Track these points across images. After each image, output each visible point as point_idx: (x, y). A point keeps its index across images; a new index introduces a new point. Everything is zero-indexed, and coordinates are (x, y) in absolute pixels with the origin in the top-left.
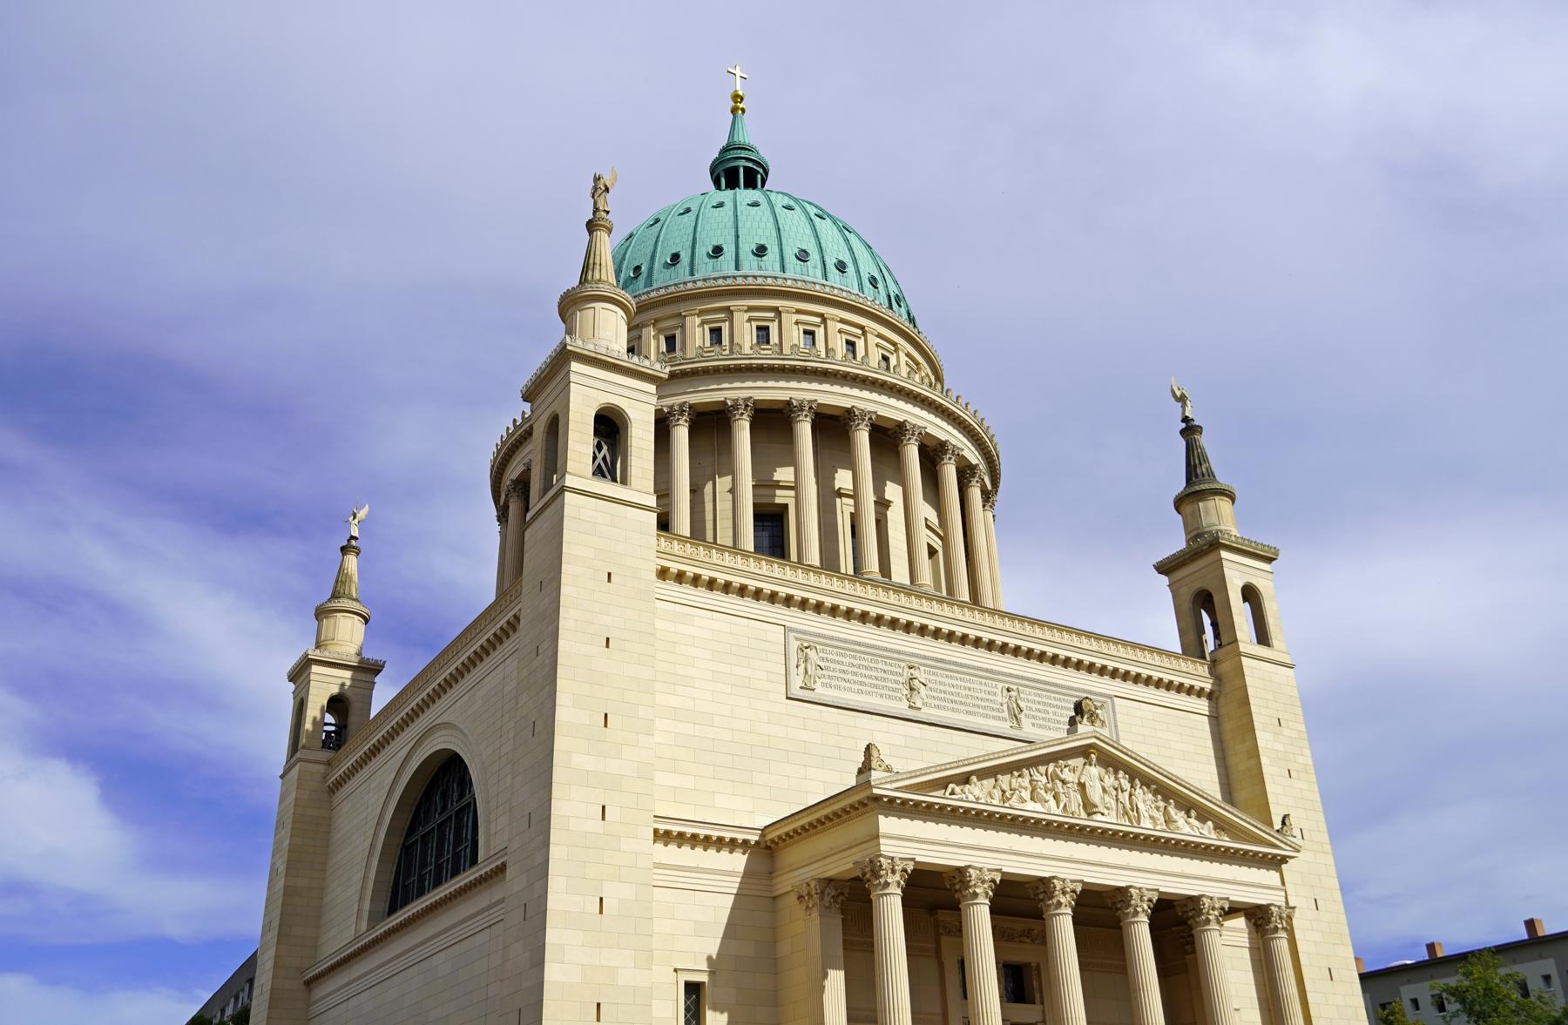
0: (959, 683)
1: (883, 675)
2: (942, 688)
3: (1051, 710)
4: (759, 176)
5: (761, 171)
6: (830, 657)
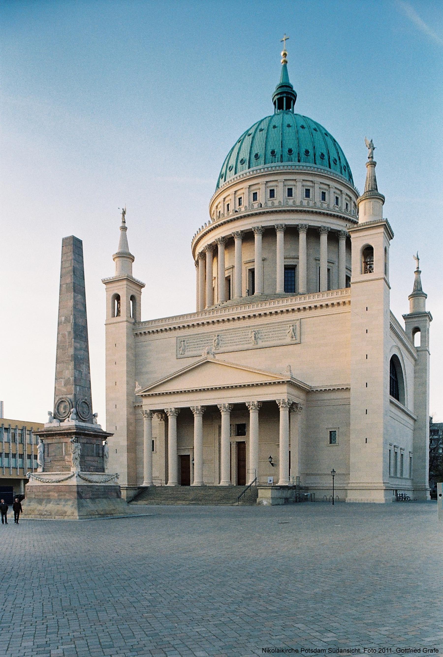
0: (234, 335)
1: (207, 341)
2: (227, 339)
3: (270, 333)
4: (285, 98)
5: (285, 95)
6: (191, 341)
